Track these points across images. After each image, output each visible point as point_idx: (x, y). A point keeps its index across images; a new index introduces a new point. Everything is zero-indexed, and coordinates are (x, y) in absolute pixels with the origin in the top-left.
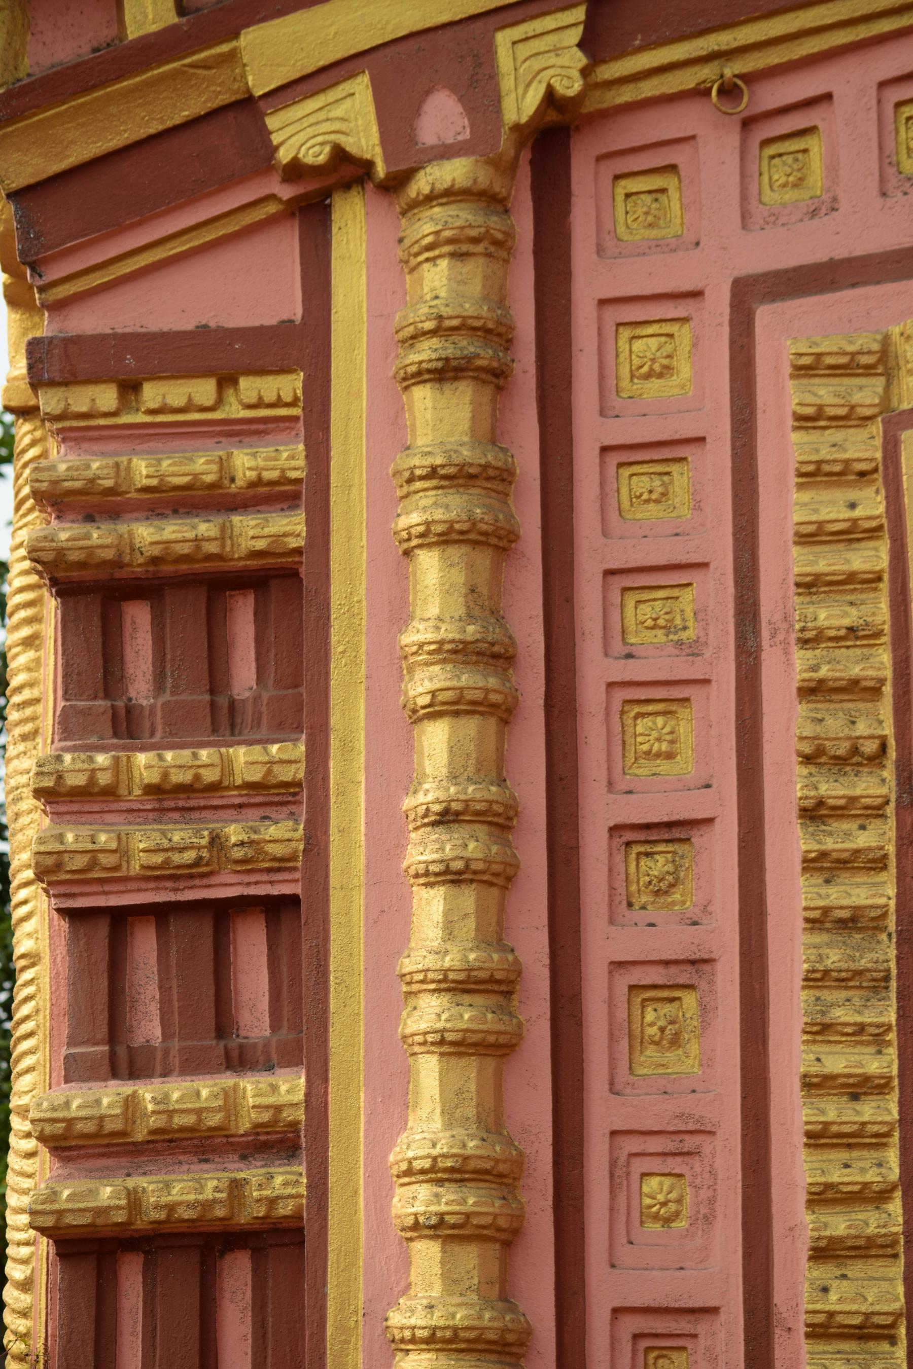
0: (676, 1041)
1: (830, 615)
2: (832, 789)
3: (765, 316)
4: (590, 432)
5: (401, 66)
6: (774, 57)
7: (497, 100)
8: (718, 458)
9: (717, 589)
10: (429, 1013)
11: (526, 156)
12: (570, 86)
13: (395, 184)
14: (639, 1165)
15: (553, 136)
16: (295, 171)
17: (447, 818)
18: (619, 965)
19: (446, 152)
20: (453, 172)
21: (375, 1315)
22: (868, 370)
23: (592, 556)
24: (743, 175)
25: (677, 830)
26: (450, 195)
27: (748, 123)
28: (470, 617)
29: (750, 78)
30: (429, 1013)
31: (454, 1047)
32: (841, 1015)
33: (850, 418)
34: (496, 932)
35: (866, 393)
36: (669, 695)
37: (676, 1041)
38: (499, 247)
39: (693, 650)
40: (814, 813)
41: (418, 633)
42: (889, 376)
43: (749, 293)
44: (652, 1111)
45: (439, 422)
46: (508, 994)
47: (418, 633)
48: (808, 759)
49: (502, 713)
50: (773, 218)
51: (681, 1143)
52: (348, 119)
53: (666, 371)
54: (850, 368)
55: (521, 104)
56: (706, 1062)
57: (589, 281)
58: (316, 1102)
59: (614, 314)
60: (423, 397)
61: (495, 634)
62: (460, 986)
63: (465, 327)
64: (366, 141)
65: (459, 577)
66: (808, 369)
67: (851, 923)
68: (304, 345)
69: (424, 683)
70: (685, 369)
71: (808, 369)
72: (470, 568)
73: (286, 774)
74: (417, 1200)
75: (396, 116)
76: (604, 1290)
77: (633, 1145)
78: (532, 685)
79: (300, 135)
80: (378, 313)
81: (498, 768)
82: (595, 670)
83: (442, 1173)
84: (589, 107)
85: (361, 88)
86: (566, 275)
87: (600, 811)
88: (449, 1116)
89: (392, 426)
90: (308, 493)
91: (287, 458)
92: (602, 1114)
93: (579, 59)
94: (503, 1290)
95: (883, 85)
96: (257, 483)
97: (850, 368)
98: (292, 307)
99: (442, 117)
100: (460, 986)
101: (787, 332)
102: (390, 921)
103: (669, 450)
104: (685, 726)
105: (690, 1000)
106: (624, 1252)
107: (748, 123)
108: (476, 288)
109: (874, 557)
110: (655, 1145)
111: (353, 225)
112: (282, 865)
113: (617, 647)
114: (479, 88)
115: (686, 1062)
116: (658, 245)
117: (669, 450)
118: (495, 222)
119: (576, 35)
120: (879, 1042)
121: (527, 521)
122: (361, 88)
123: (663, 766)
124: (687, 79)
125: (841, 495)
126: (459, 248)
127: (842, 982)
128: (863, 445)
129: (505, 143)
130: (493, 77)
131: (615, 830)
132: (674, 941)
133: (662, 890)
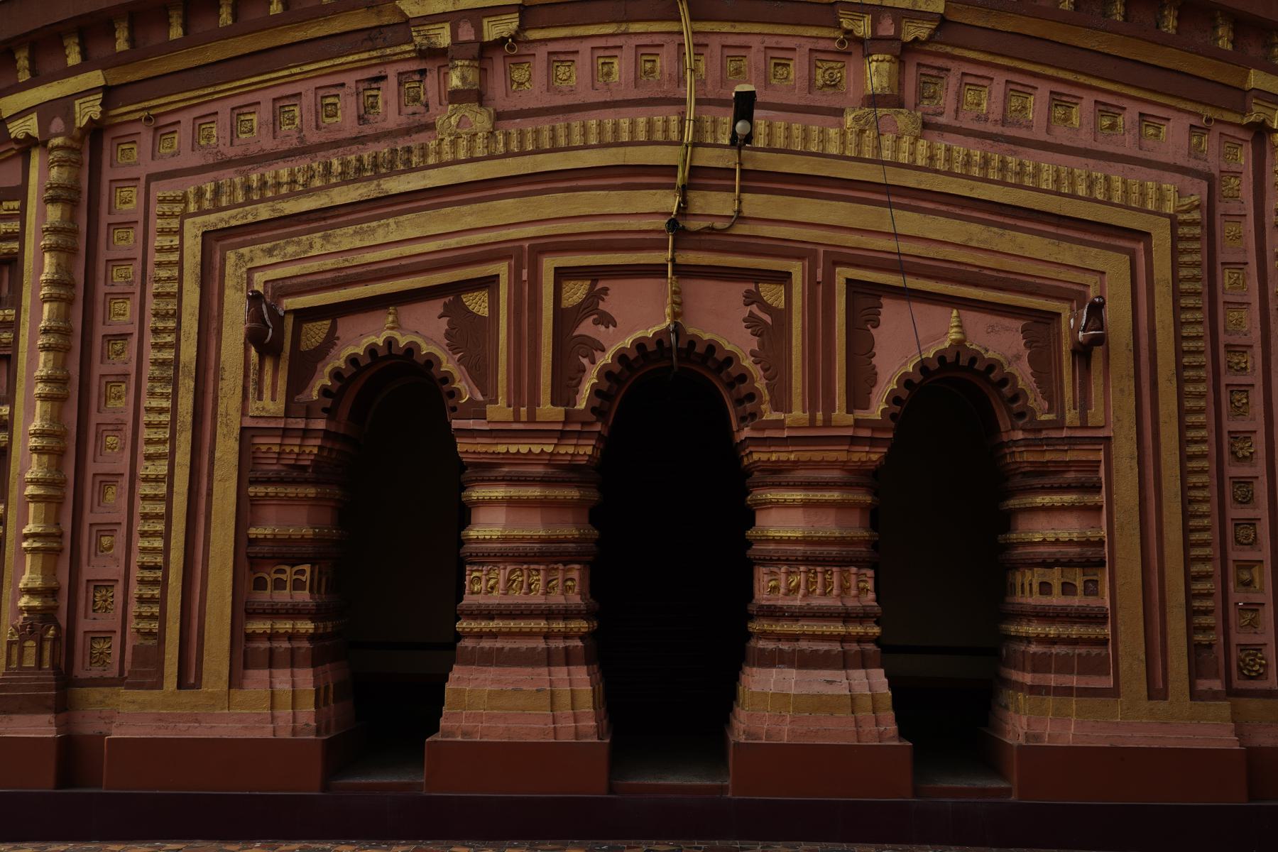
0: (120, 397)
1: (164, 274)
2: (160, 325)
3: (153, 185)
4: (105, 218)
5: (45, 111)
6: (162, 110)
7: (74, 120)
8: (140, 227)
9: (137, 265)
10: (40, 388)
11: (87, 138)
12: (97, 116)
13: (45, 144)
14: (106, 433)
15: (95, 131)
16: (16, 140)
17: (46, 331)
18: (102, 376)
19: (57, 135)
20: (58, 141)
21: (21, 475)
22: (180, 202)
23: (103, 255)
24: (154, 144)
25: (124, 336)
26: (58, 148)
27: (156, 129)
28: (57, 273)
29: (156, 116)
30: (40, 388)
31: (44, 398)
32: (158, 390)
33: (173, 215)
34: (61, 365)
35: (178, 209)
36: (125, 296)
37: (120, 397)
38: (77, 164)
39: (131, 284)
40: (156, 331)
41: (43, 277)
42: (187, 204)
43: (151, 178)
44: (107, 417)
45: (54, 214)
46: (65, 384)
47: (43, 277)
48: (155, 316)
49: (69, 302)
50: (162, 157)
51: (117, 427)
52: (31, 126)
53: (130, 201)
54: (174, 201)
55: (82, 121)
56: (127, 404)
57: (107, 174)
58: (11, 414)
59: (115, 185)
60: (49, 207)
61: (66, 277)
62: (47, 380)
63: (59, 187)
64: (35, 132)
65: (54, 261)
66: (163, 201)
67: (162, 364)
68: (20, 193)
69: (45, 291)
70: (135, 201)
71: (163, 201)
72: (58, 258)
73: (9, 319)
74: (33, 442)
75: (44, 124)
76: (92, 468)
77: (104, 427)
78: (79, 293)
79: (17, 129)
80: (40, 183)
81: (67, 318)
82: (102, 289)
83: (40, 434)
84: (107, 123)
85: (35, 116)
86: (100, 173)
87: (100, 330)
88: (42, 419)
89: (42, 215)
90: (19, 236)
91: (14, 226)
92: (95, 418)
93: (100, 109)
94: (59, 467)
95: (195, 119)
96: (6, 233)
97: (174, 201)
98: (19, 182)
99: (57, 125)
100: (47, 380)
101: (160, 190)
102: (32, 362)
103: (129, 224)
104: (128, 305)
105: (124, 386)
106: (99, 458)
107: (156, 129)
108: (65, 176)
109: (174, 257)
110: (110, 427)
111: (36, 159)
112: (7, 345)
113: (109, 282)
114: (69, 117)
115: (119, 404)
116: (129, 165)
117: (129, 224)
118: (73, 157)
119: (99, 102)
120: (167, 398)
121: (81, 244)
122: (35, 116)
123: (121, 318)
124: (137, 116)
125: (169, 238)
126: (61, 163)
127: (159, 381)
128: (175, 224)
129: (76, 133)
130: (73, 113)
131: (104, 336)
132: (119, 369)
133: (118, 354)
